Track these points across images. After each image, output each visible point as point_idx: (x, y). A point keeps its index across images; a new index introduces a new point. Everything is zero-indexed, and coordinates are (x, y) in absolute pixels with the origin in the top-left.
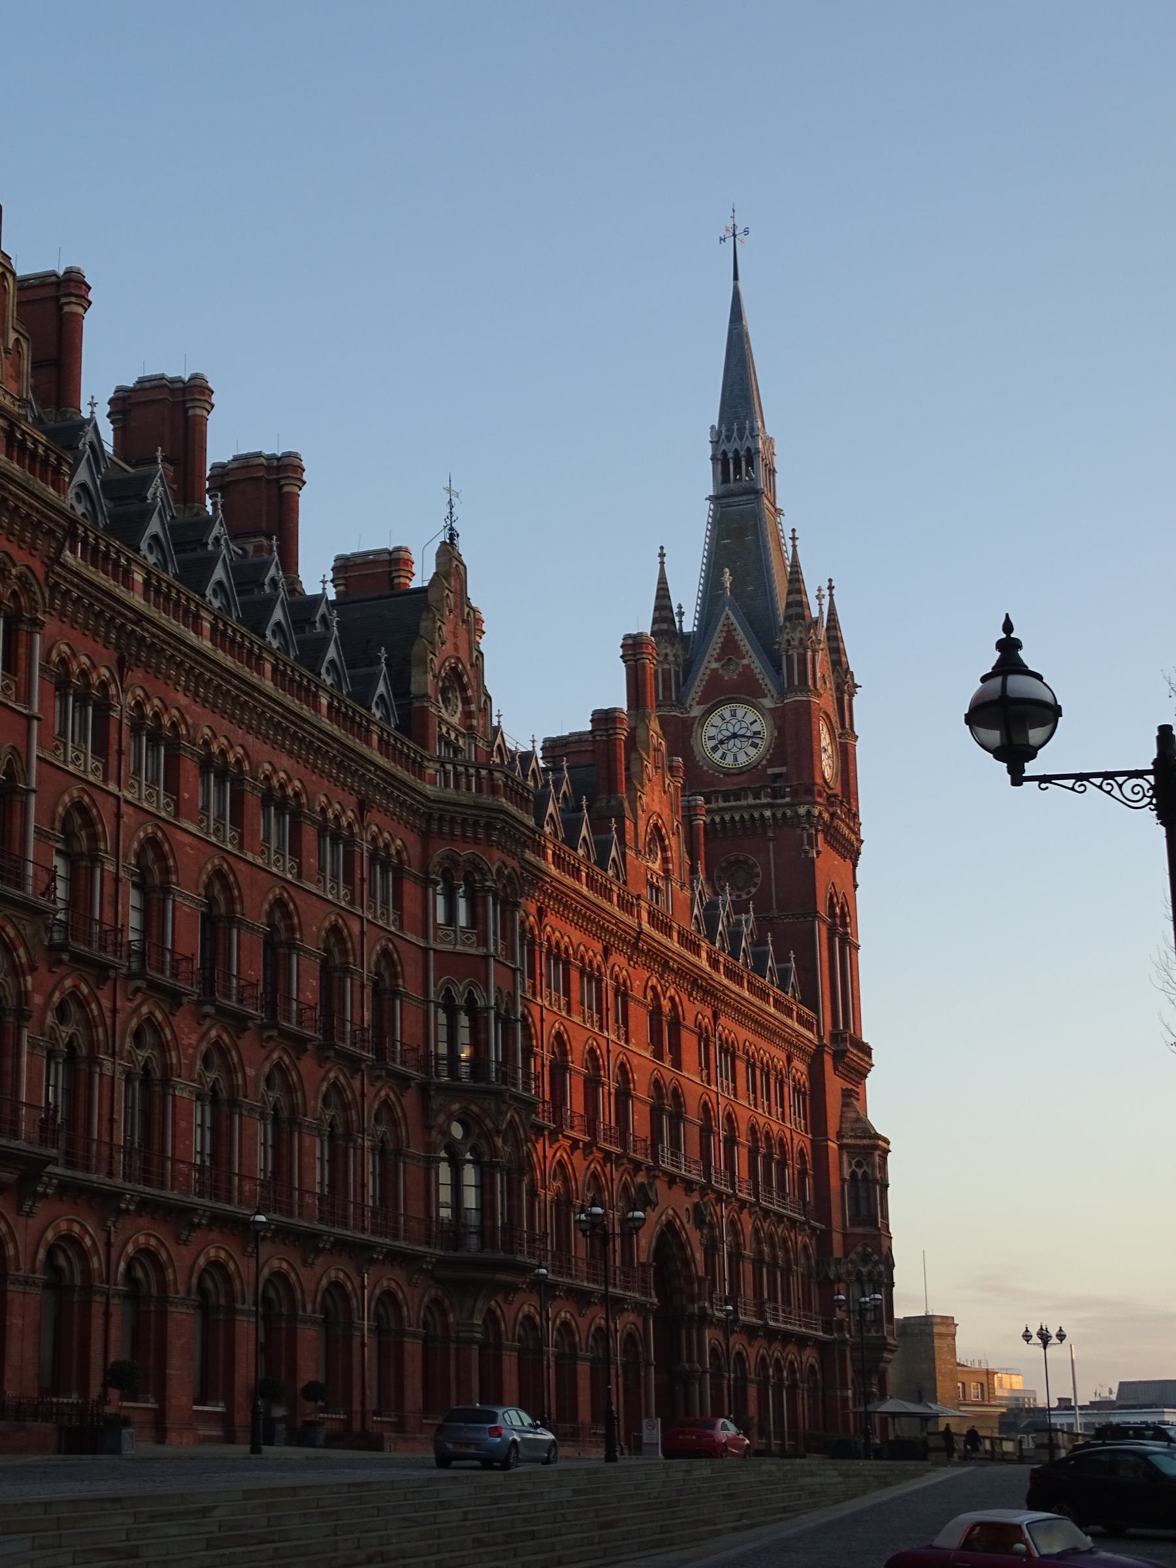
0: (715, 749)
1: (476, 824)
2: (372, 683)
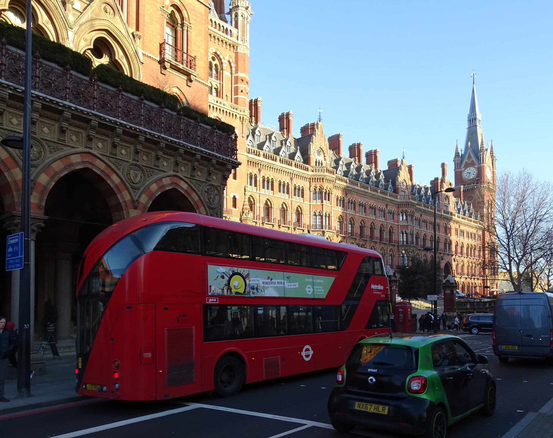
0: (466, 176)
1: (406, 205)
2: (388, 185)
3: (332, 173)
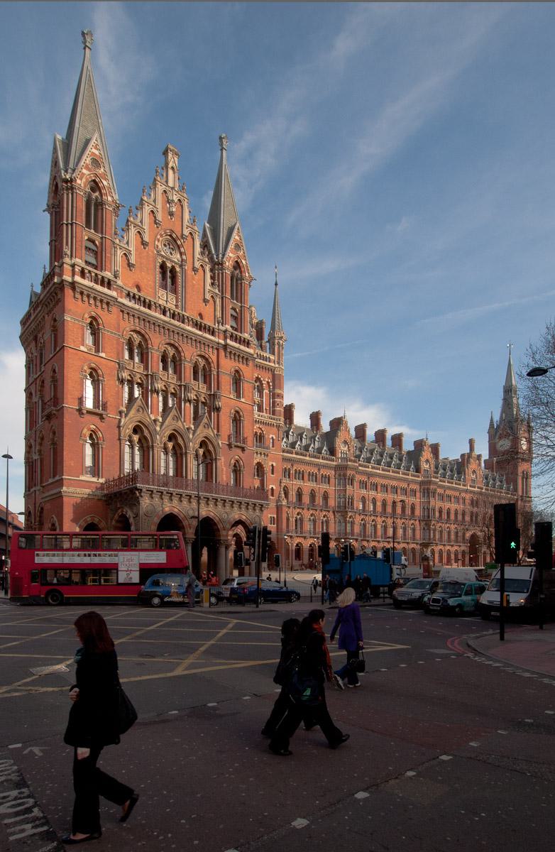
3: (355, 462)
